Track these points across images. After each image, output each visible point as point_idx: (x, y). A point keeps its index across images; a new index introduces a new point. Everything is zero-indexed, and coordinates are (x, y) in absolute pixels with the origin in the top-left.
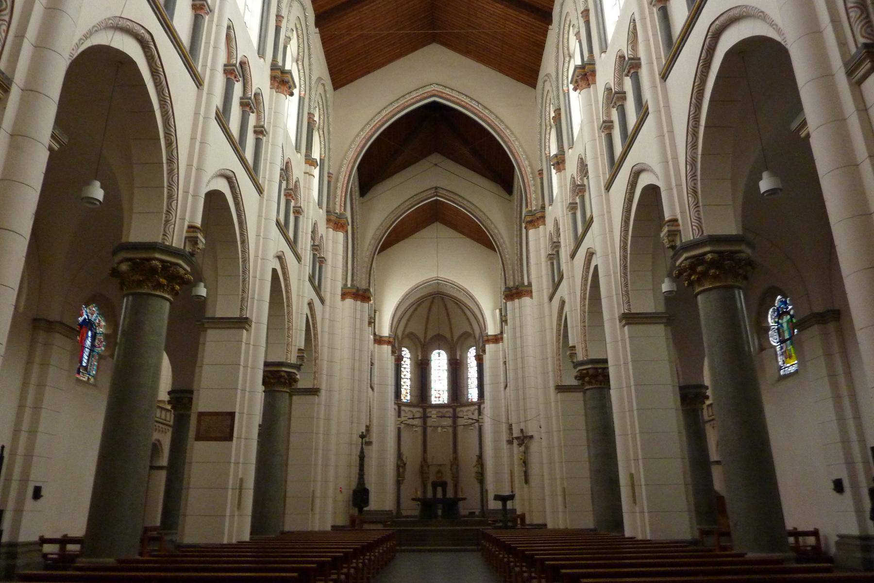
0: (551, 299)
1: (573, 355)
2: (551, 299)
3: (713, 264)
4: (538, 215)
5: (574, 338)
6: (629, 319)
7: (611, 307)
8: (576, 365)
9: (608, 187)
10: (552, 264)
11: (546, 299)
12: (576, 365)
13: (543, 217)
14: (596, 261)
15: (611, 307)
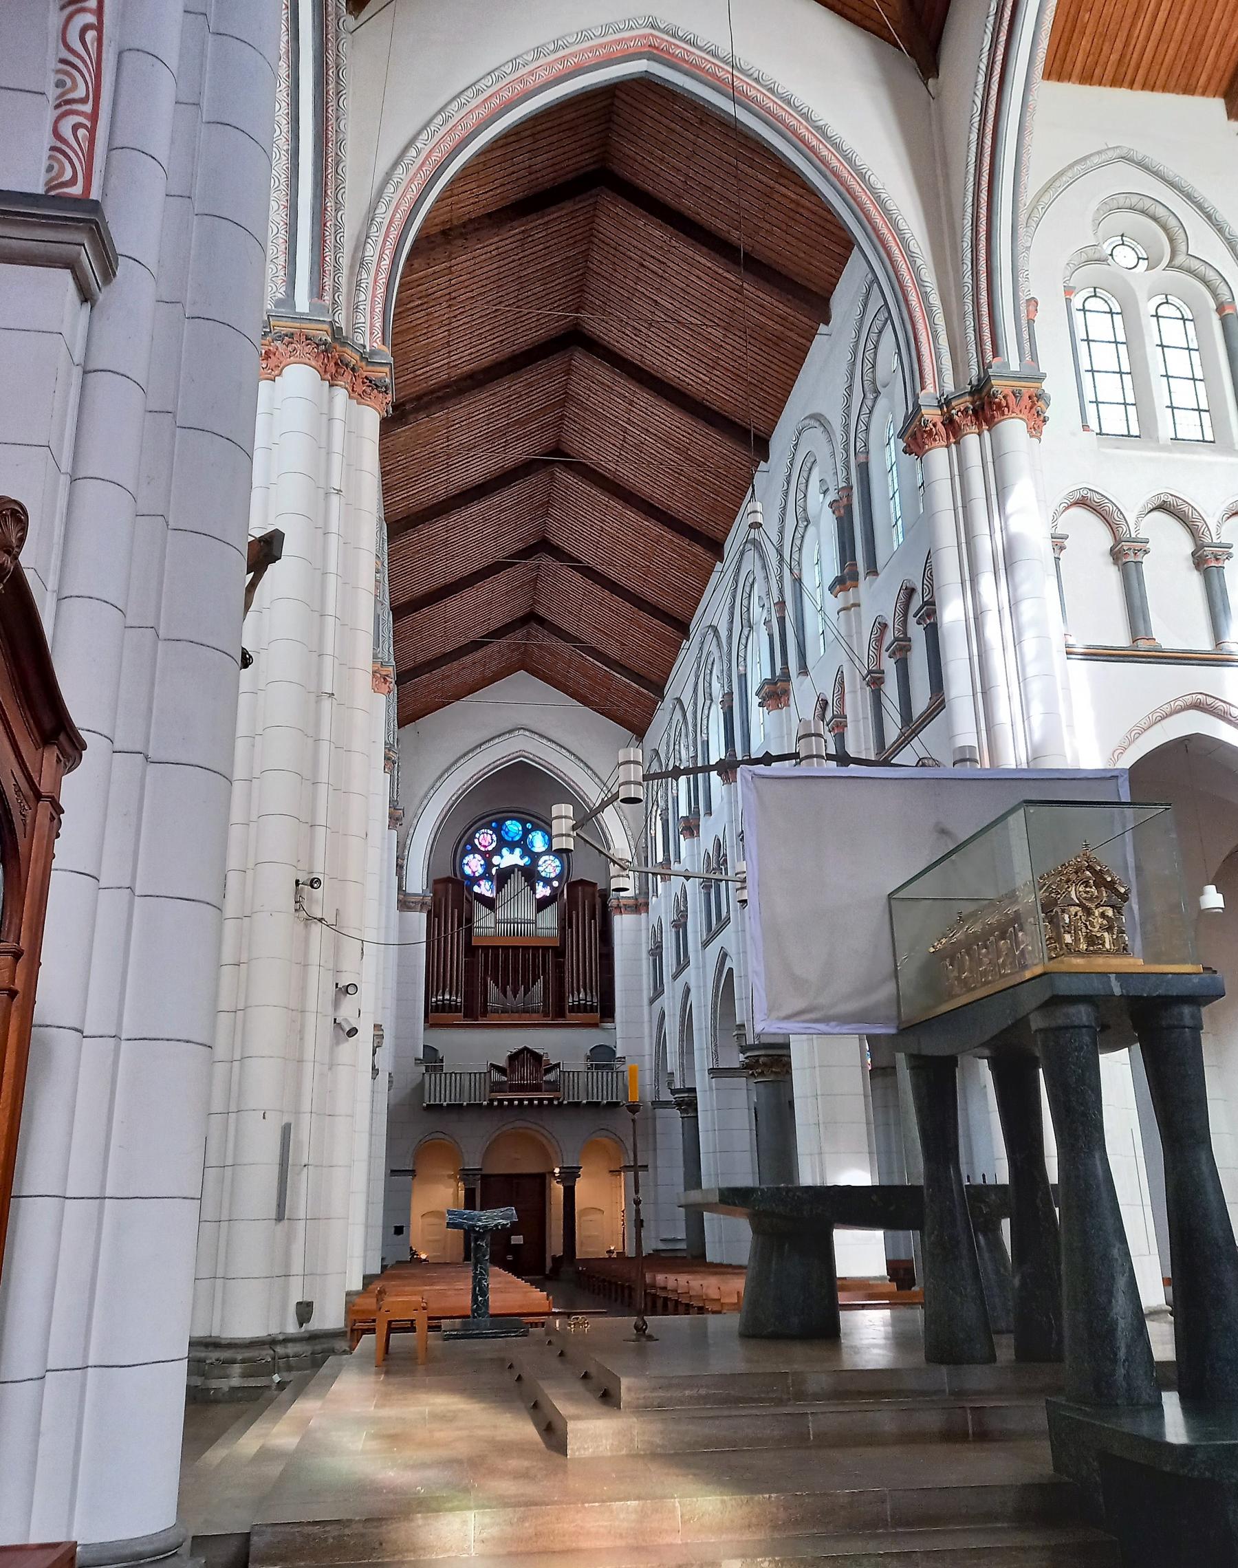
0: (652, 1001)
1: (670, 1083)
2: (652, 1001)
3: (765, 1064)
4: (641, 900)
5: (673, 1062)
6: (715, 1072)
7: (702, 1060)
8: (673, 1092)
9: (705, 944)
10: (655, 961)
11: (646, 1001)
12: (673, 1092)
13: (647, 904)
14: (693, 997)
15: (702, 1060)
